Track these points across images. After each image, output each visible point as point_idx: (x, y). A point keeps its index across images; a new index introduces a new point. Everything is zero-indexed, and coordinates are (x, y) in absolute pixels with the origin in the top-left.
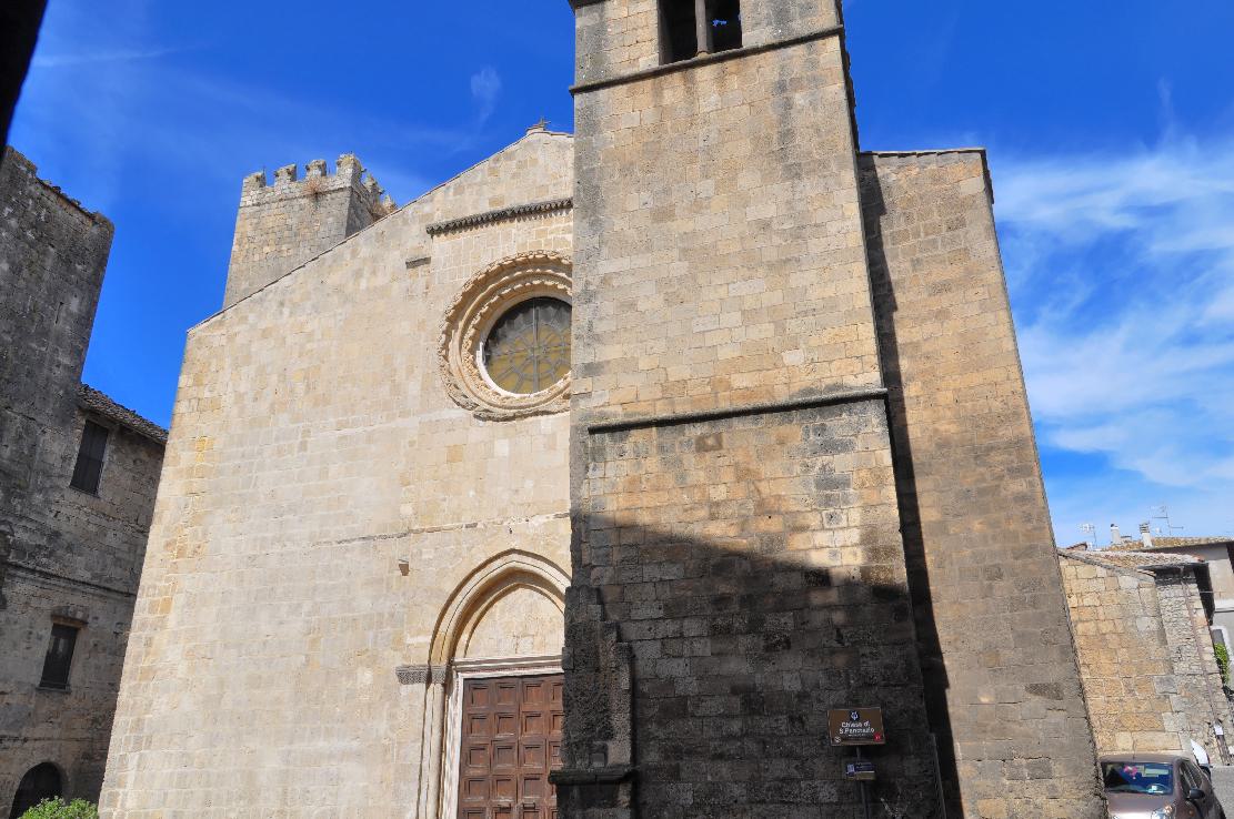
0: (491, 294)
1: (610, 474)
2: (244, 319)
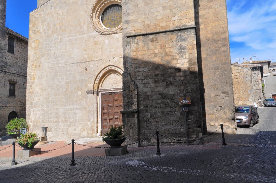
0: (102, 4)
2: (43, 10)
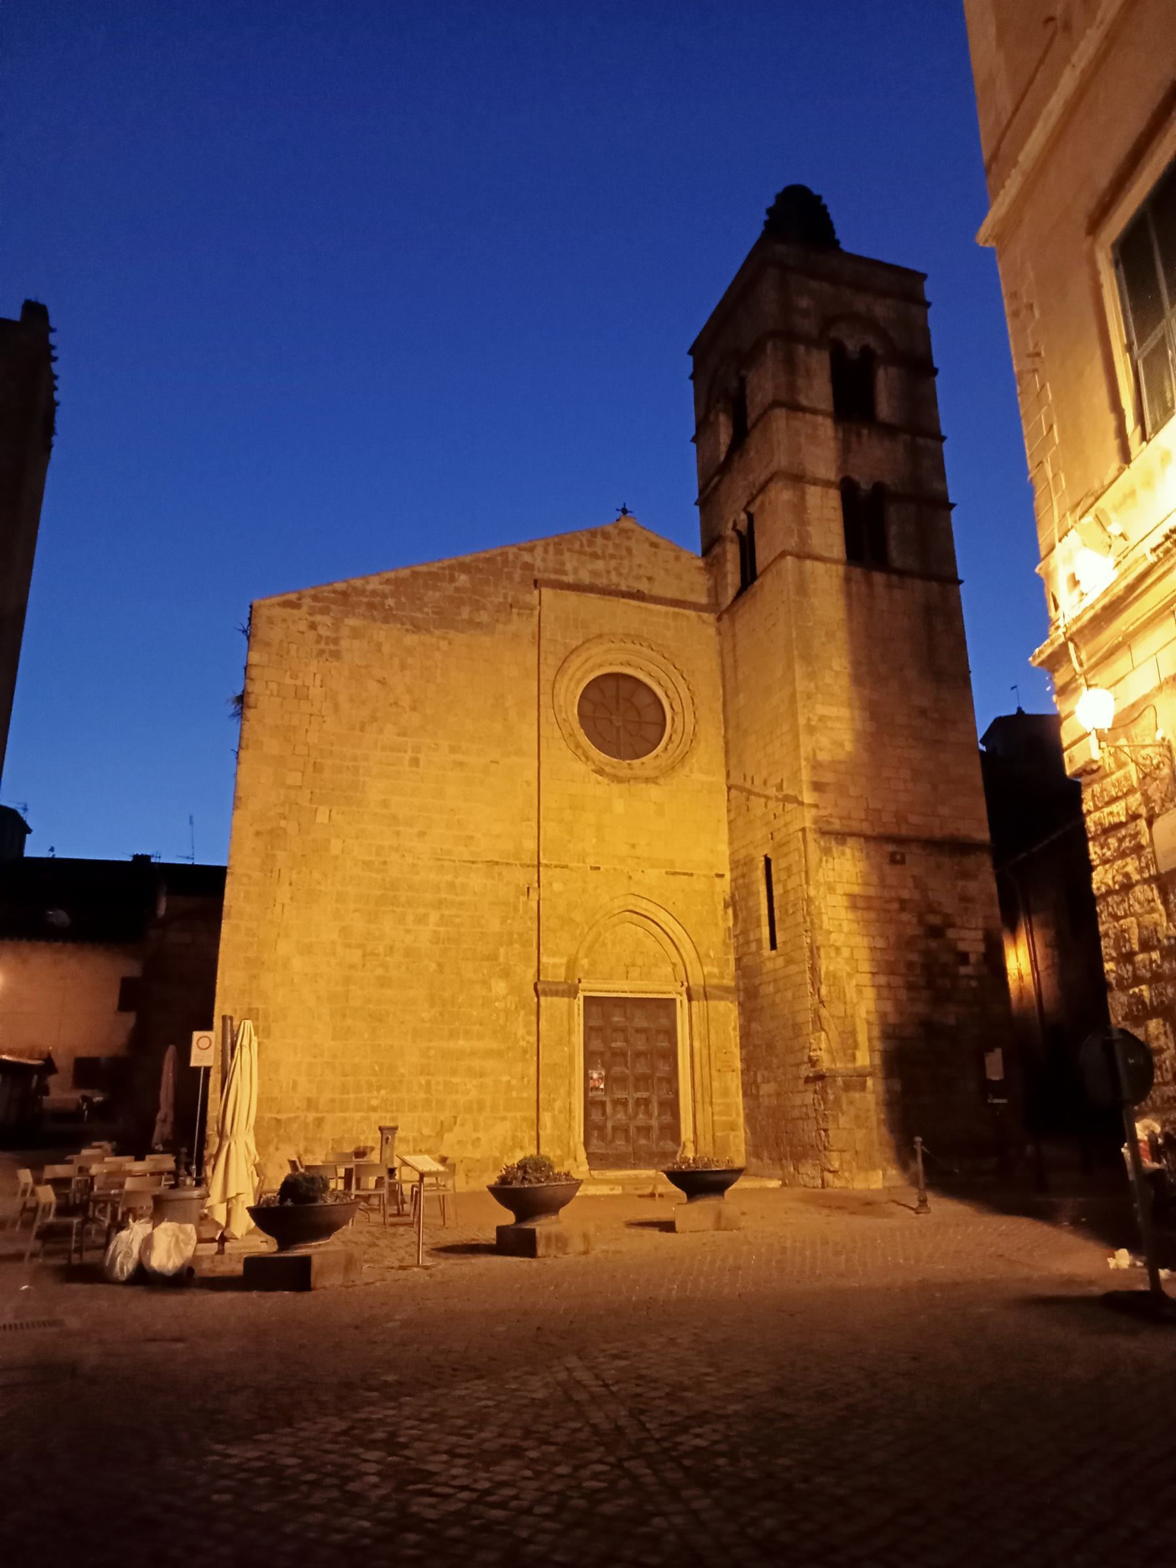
1: (837, 867)
